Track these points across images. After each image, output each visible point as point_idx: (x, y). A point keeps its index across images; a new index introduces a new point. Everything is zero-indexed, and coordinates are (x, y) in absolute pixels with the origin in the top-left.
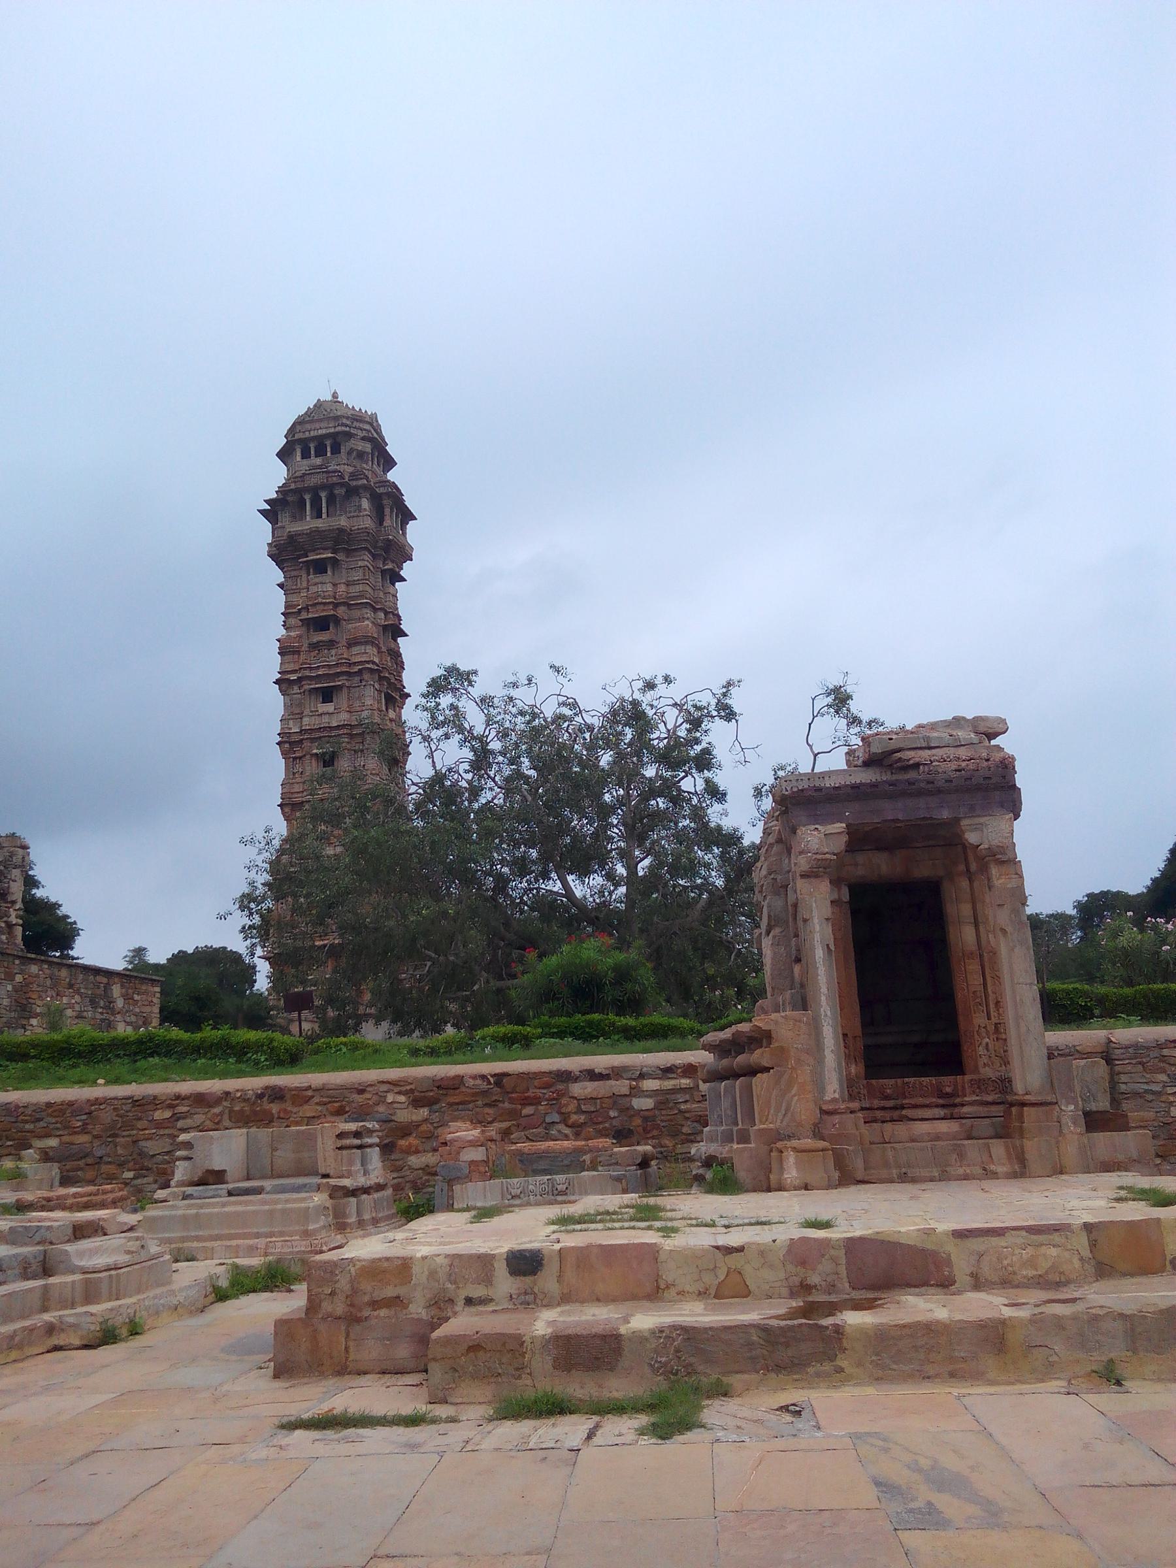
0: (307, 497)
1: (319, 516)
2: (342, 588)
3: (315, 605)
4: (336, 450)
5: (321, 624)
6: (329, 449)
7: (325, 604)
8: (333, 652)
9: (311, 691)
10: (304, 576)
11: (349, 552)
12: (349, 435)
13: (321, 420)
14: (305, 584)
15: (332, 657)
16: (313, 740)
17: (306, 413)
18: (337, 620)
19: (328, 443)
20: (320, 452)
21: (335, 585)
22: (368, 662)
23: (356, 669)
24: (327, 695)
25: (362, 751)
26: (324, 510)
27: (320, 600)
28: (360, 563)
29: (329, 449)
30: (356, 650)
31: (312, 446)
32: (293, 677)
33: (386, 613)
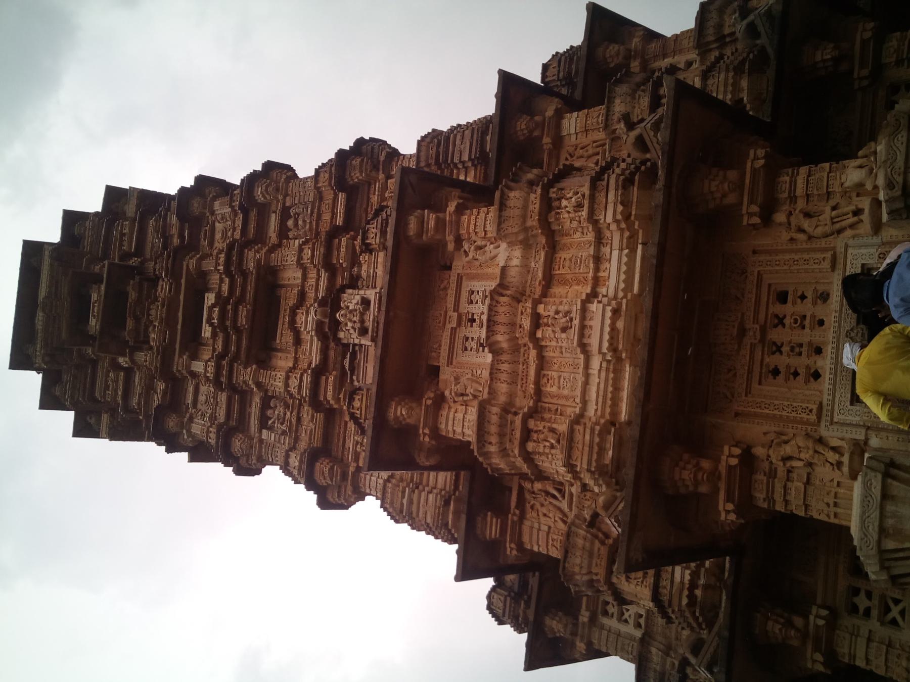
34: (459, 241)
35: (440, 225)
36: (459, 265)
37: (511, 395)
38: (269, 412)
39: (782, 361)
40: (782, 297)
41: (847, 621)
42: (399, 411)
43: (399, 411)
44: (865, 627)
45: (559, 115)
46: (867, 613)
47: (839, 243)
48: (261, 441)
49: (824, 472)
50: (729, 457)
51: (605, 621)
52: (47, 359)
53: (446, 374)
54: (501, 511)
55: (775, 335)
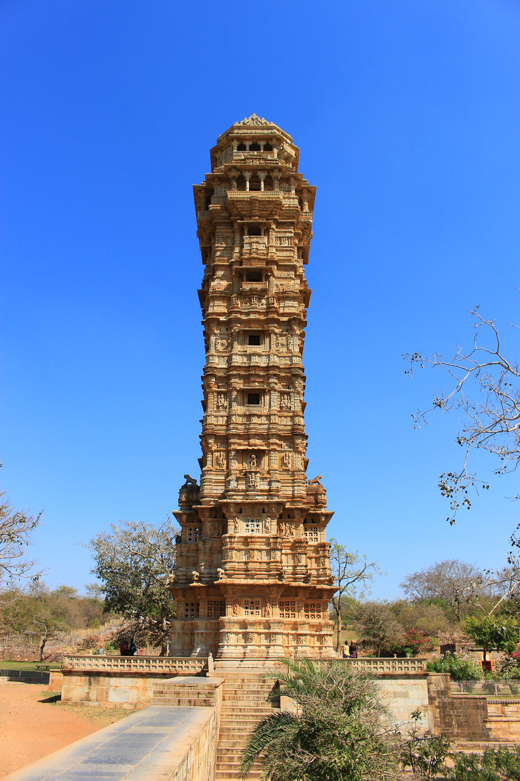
0: (248, 175)
1: (259, 189)
2: (274, 250)
3: (249, 259)
6: (262, 148)
8: (264, 301)
9: (238, 333)
12: (280, 140)
13: (255, 128)
15: (261, 305)
16: (240, 377)
21: (267, 248)
22: (294, 314)
23: (285, 319)
24: (255, 339)
25: (288, 394)
27: (254, 255)
28: (288, 235)
29: (262, 148)
32: (222, 319)
33: (301, 281)
46: (209, 604)
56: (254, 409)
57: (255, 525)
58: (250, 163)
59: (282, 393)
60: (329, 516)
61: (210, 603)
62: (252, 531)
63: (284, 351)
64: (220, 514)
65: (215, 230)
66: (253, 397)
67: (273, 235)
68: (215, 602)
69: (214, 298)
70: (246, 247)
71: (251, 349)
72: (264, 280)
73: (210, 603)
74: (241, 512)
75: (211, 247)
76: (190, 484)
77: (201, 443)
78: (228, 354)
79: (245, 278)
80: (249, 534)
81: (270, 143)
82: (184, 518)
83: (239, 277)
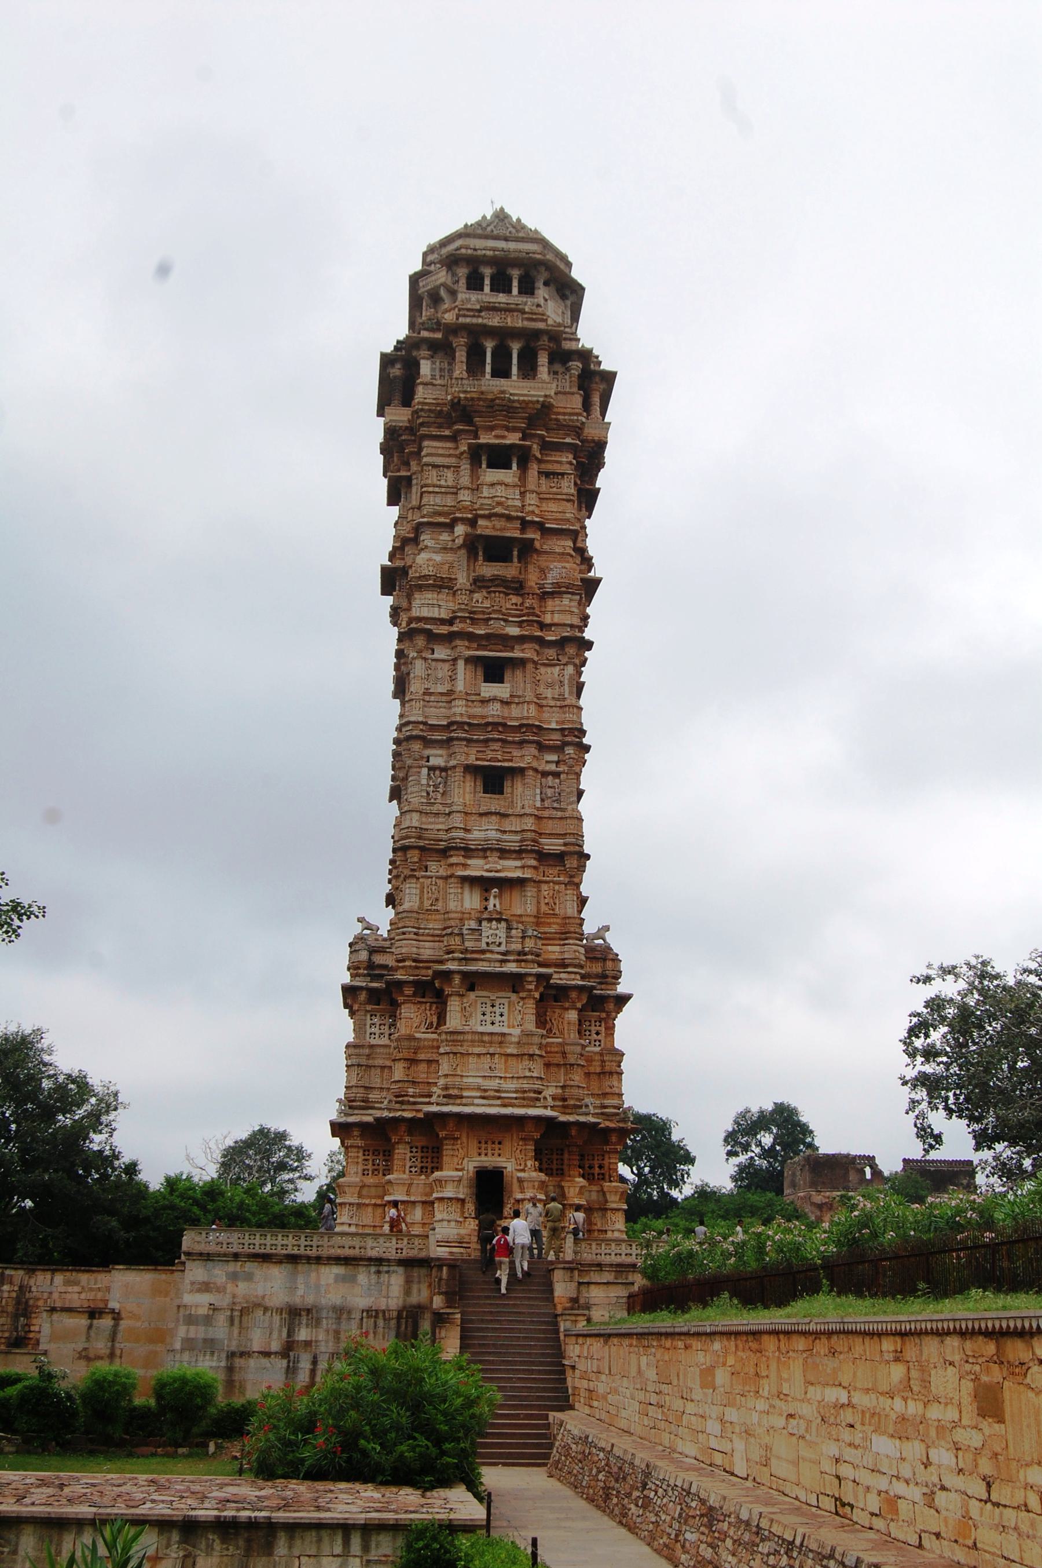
0: (489, 346)
4: (527, 288)
5: (496, 549)
7: (509, 518)
9: (468, 660)
10: (465, 466)
11: (547, 447)
14: (465, 480)
17: (479, 224)
18: (527, 549)
19: (515, 273)
20: (501, 284)
22: (572, 626)
25: (556, 775)
26: (515, 370)
27: (499, 510)
30: (550, 604)
31: (487, 272)
34: (523, 998)
35: (530, 991)
36: (514, 997)
37: (467, 1041)
38: (437, 773)
39: (483, 1146)
40: (500, 1143)
41: (408, 1147)
42: (457, 979)
43: (457, 979)
44: (408, 1151)
45: (576, 1009)
47: (513, 1160)
48: (420, 767)
49: (456, 1160)
50: (457, 1134)
51: (368, 1017)
52: (456, 400)
53: (472, 995)
54: (414, 995)
55: (489, 1142)
56: (493, 803)
57: (497, 1014)
58: (494, 321)
59: (545, 774)
60: (623, 1000)
61: (414, 1150)
62: (493, 1023)
63: (549, 696)
64: (433, 990)
65: (420, 449)
66: (494, 780)
67: (534, 469)
68: (422, 1148)
69: (420, 588)
70: (486, 492)
71: (490, 690)
72: (515, 560)
73: (414, 1150)
74: (472, 988)
75: (409, 479)
76: (368, 932)
77: (392, 862)
78: (448, 698)
79: (481, 553)
80: (490, 1029)
81: (533, 273)
82: (363, 996)
83: (469, 552)
